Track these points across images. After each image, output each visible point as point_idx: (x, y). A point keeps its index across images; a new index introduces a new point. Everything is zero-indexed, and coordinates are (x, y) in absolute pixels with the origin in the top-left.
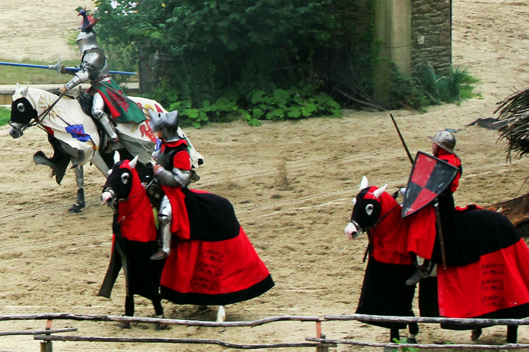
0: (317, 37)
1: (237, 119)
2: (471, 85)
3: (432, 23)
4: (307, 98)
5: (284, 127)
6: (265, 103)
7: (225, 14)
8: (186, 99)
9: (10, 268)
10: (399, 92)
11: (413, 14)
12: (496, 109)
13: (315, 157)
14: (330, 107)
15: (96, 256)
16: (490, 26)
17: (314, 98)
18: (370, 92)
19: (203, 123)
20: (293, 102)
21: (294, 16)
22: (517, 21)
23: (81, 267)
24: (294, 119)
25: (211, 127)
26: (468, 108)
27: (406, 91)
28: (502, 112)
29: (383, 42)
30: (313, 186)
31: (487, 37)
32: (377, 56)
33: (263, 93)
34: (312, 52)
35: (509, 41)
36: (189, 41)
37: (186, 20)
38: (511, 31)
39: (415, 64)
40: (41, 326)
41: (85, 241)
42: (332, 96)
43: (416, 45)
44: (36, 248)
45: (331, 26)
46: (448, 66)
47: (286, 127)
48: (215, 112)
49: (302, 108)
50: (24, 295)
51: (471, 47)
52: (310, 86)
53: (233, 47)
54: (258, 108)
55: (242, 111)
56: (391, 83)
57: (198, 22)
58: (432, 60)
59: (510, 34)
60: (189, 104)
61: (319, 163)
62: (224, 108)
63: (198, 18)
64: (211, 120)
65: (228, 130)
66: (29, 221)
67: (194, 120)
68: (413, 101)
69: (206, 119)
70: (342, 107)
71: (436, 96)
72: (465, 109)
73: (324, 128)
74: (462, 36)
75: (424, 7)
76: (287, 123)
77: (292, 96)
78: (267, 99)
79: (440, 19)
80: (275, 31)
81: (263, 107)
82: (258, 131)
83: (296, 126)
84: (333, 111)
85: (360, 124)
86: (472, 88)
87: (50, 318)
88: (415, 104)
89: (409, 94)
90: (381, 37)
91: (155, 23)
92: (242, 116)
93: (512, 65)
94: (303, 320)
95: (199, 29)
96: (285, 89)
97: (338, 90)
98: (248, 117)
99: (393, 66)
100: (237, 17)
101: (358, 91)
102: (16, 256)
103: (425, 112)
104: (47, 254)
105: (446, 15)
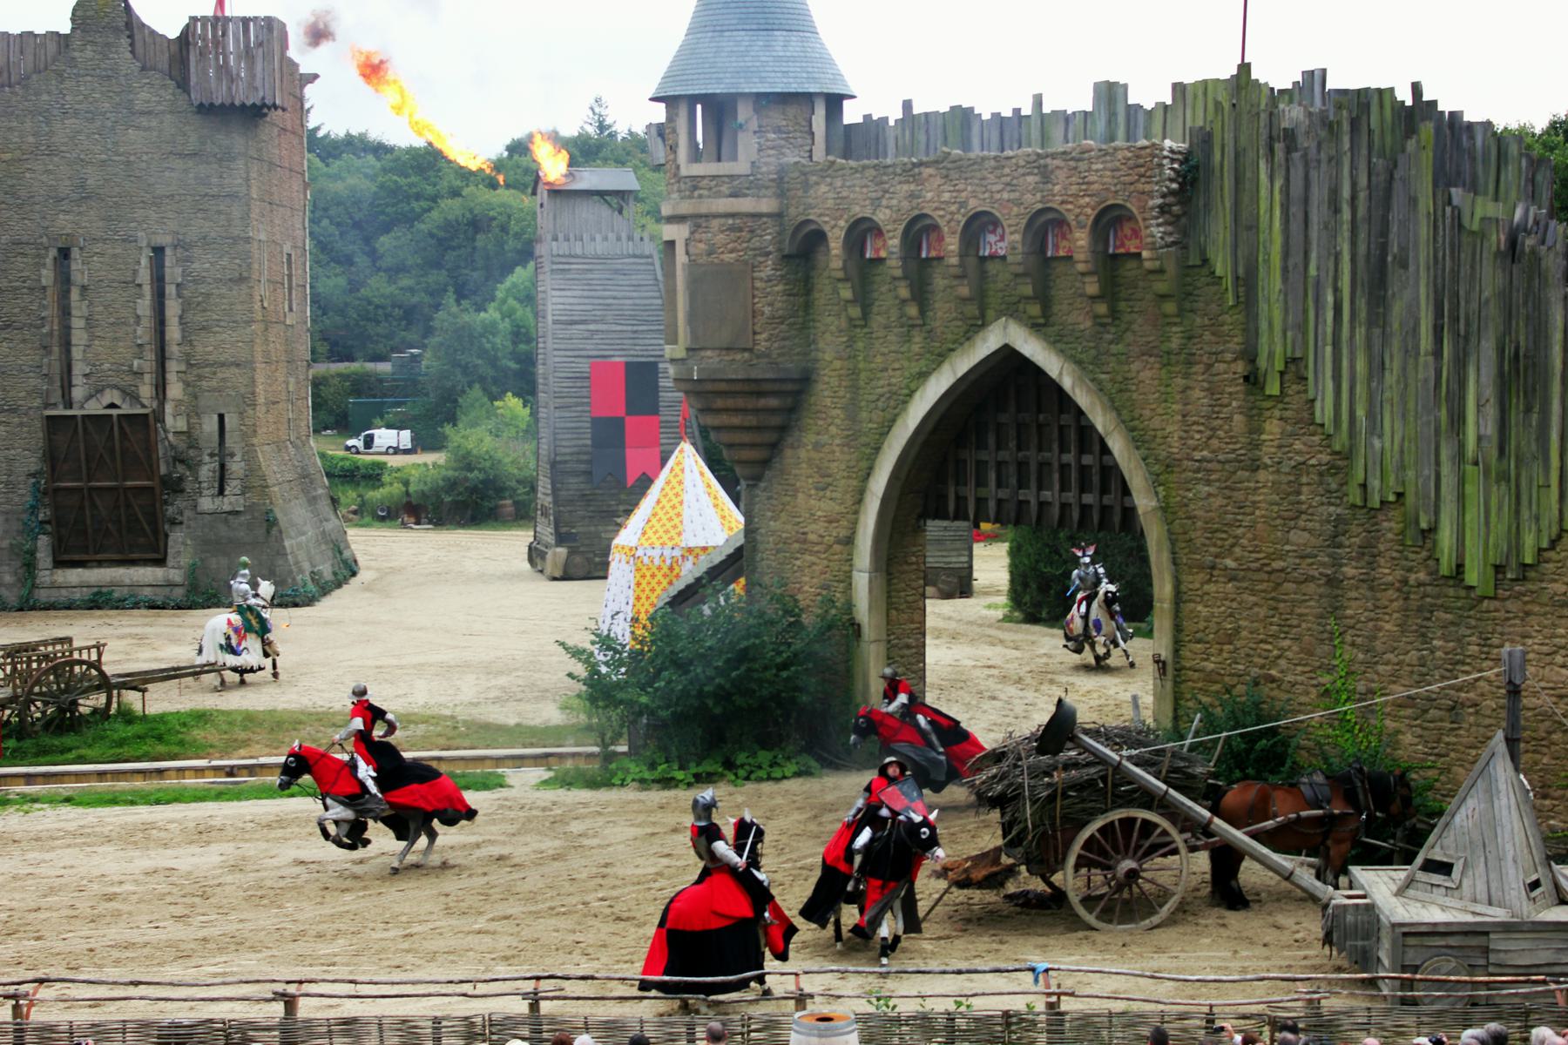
4: (789, 758)
5: (767, 787)
9: (499, 929)
13: (797, 816)
15: (585, 916)
19: (689, 785)
23: (570, 927)
24: (777, 780)
30: (794, 844)
34: (794, 715)
35: (979, 703)
36: (677, 704)
37: (673, 685)
40: (529, 986)
41: (574, 902)
44: (525, 909)
45: (812, 690)
50: (513, 957)
53: (718, 711)
55: (726, 772)
57: (685, 687)
60: (676, 767)
61: (800, 822)
64: (697, 782)
66: (519, 883)
69: (693, 780)
70: (822, 767)
76: (770, 783)
77: (775, 757)
78: (751, 760)
79: (915, 682)
80: (758, 694)
81: (747, 767)
87: (538, 978)
93: (983, 725)
94: (783, 974)
95: (685, 693)
98: (733, 778)
102: (506, 918)
104: (537, 915)
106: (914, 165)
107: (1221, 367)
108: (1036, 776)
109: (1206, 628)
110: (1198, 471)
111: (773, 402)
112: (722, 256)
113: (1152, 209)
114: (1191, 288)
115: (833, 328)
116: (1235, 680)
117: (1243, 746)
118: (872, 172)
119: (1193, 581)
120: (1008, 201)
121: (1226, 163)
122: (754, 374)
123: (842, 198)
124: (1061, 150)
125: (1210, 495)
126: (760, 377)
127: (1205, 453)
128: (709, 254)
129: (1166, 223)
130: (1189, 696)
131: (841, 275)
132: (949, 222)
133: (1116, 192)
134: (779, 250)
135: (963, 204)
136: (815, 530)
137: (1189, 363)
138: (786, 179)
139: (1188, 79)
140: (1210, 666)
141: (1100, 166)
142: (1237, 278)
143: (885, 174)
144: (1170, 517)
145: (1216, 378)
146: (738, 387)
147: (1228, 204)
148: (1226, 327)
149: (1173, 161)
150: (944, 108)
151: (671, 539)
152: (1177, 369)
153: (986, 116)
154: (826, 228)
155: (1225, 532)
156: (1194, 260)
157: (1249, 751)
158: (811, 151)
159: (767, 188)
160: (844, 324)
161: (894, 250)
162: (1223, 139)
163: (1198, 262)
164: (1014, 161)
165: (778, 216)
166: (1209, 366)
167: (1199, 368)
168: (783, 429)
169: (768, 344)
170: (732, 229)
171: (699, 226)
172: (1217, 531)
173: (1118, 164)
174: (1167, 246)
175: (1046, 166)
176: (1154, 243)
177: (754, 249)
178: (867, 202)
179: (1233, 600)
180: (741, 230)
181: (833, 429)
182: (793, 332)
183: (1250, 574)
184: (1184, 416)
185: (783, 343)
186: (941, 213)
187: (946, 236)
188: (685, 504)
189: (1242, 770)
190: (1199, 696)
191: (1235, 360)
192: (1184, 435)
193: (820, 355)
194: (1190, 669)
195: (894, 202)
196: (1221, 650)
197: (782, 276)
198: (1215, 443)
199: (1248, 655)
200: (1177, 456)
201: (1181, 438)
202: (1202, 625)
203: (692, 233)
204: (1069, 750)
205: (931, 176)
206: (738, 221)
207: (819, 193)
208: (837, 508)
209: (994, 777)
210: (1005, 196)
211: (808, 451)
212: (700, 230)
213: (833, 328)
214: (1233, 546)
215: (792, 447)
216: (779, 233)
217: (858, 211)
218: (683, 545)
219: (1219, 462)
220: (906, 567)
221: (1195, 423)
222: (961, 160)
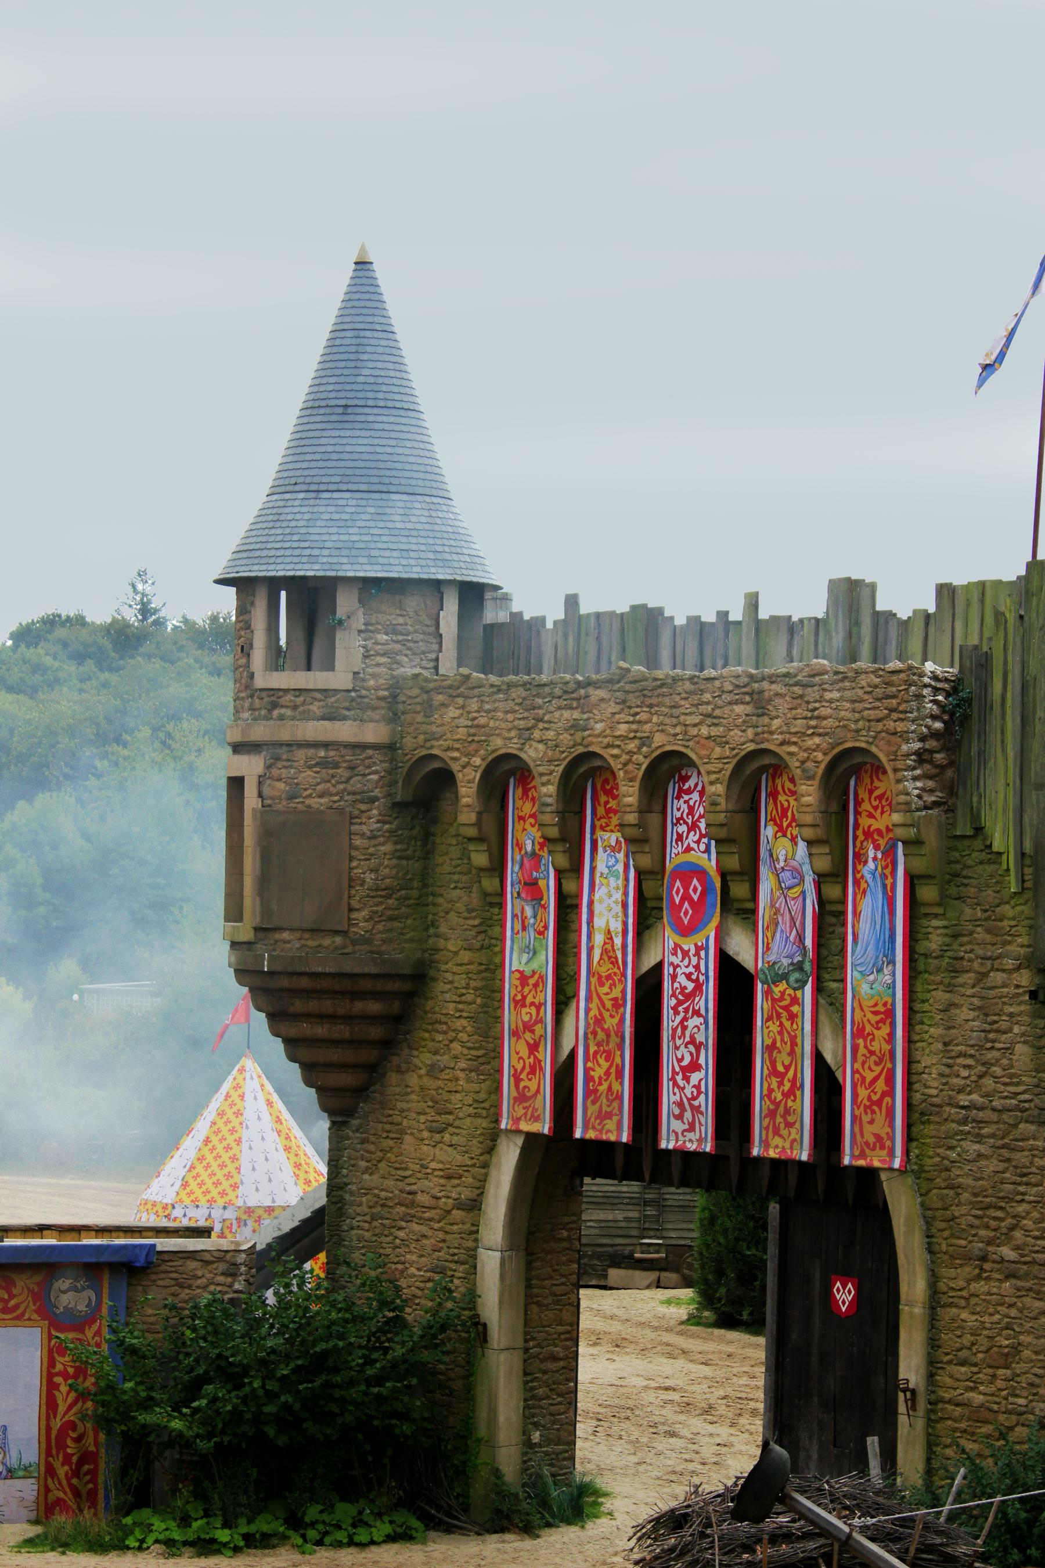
0: (397, 1431)
1: (284, 1545)
2: (600, 1500)
3: (552, 1415)
4: (380, 1515)
6: (324, 1522)
7: (272, 1396)
8: (215, 1515)
10: (505, 1509)
11: (525, 1400)
12: (631, 1534)
14: (410, 1528)
16: (628, 1418)
17: (389, 1516)
18: (466, 1508)
19: (237, 1550)
20: (361, 1521)
21: (366, 1399)
22: (663, 1412)
25: (249, 1555)
26: (596, 1532)
27: (513, 1508)
28: (639, 1539)
29: (486, 1439)
31: (623, 1433)
32: (476, 1458)
33: (320, 1507)
34: (389, 1452)
36: (223, 1432)
38: (655, 1425)
39: (527, 1470)
42: (414, 1513)
43: (528, 1444)
46: (571, 1473)
47: (350, 1557)
48: (254, 1535)
49: (374, 1530)
51: (602, 1447)
52: (385, 1499)
53: (282, 1441)
54: (314, 1528)
55: (290, 1533)
56: (493, 1496)
58: (549, 1465)
59: (654, 1430)
62: (266, 1528)
63: (235, 1400)
64: (248, 1546)
65: (270, 1560)
67: (225, 1545)
68: (522, 1521)
69: (242, 1543)
70: (428, 1528)
71: (553, 1516)
72: (590, 1533)
73: (401, 1559)
74: (590, 1432)
75: (540, 1392)
76: (352, 1550)
77: (360, 1513)
78: (325, 1517)
79: (562, 1408)
80: (339, 1420)
81: (320, 1527)
82: (312, 1561)
83: (363, 1555)
84: (415, 1534)
85: (450, 1553)
86: (602, 1504)
88: (525, 1526)
89: (519, 1512)
90: (482, 1432)
91: (176, 1408)
92: (291, 1541)
93: (656, 1473)
95: (236, 1416)
96: (351, 1502)
97: (422, 1505)
98: (300, 1541)
99: (497, 1473)
100: (290, 1400)
101: (450, 1506)
103: (538, 1536)
105: (570, 1403)
106: (579, 684)
107: (998, 977)
108: (731, 1551)
109: (973, 1344)
110: (964, 1121)
111: (374, 1007)
112: (308, 802)
113: (907, 755)
114: (958, 866)
115: (460, 906)
116: (1014, 1418)
117: (1023, 1515)
118: (521, 692)
119: (955, 1277)
120: (709, 738)
121: (1009, 696)
122: (349, 966)
123: (478, 726)
124: (784, 670)
125: (980, 1156)
126: (356, 970)
127: (975, 1097)
128: (291, 798)
129: (925, 776)
130: (949, 1441)
131: (472, 832)
132: (625, 765)
133: (857, 731)
134: (389, 795)
135: (645, 741)
136: (427, 1188)
137: (955, 971)
138: (401, 698)
139: (959, 579)
140: (977, 1398)
141: (836, 695)
142: (1023, 854)
143: (538, 695)
144: (925, 1185)
145: (992, 993)
146: (325, 984)
147: (1011, 754)
148: (1006, 923)
149: (936, 690)
150: (623, 608)
151: (223, 1194)
152: (938, 978)
153: (680, 621)
154: (455, 767)
155: (1001, 1208)
156: (963, 828)
157: (1031, 1523)
158: (437, 659)
159: (374, 709)
160: (475, 900)
161: (549, 800)
162: (1005, 663)
163: (969, 832)
164: (717, 683)
165: (390, 748)
166: (985, 975)
167: (968, 978)
168: (388, 1045)
169: (368, 925)
170: (324, 764)
171: (278, 759)
172: (990, 1206)
173: (860, 692)
174: (926, 808)
175: (761, 692)
176: (907, 803)
177: (354, 794)
178: (513, 733)
179: (1010, 1306)
180: (336, 766)
181: (456, 1047)
182: (404, 909)
183: (1035, 1269)
184: (946, 1044)
185: (389, 925)
186: (615, 751)
187: (621, 783)
188: (245, 1145)
189: (1022, 1550)
190: (963, 1442)
191: (1018, 968)
192: (947, 1071)
193: (441, 943)
194: (949, 1402)
195: (551, 734)
196: (994, 1376)
197: (390, 831)
198: (988, 1083)
199: (1032, 1385)
200: (935, 1100)
201: (942, 1075)
202: (967, 1339)
203: (268, 767)
204: (779, 1514)
205: (602, 700)
206: (332, 753)
207: (447, 718)
208: (459, 1158)
209: (672, 1550)
210: (704, 731)
211: (420, 1077)
212: (280, 764)
213: (460, 906)
214: (1012, 1228)
215: (399, 1071)
216: (389, 772)
217: (499, 745)
218: (240, 1203)
219: (994, 1110)
220: (554, 1245)
221: (961, 1055)
222: (645, 679)
